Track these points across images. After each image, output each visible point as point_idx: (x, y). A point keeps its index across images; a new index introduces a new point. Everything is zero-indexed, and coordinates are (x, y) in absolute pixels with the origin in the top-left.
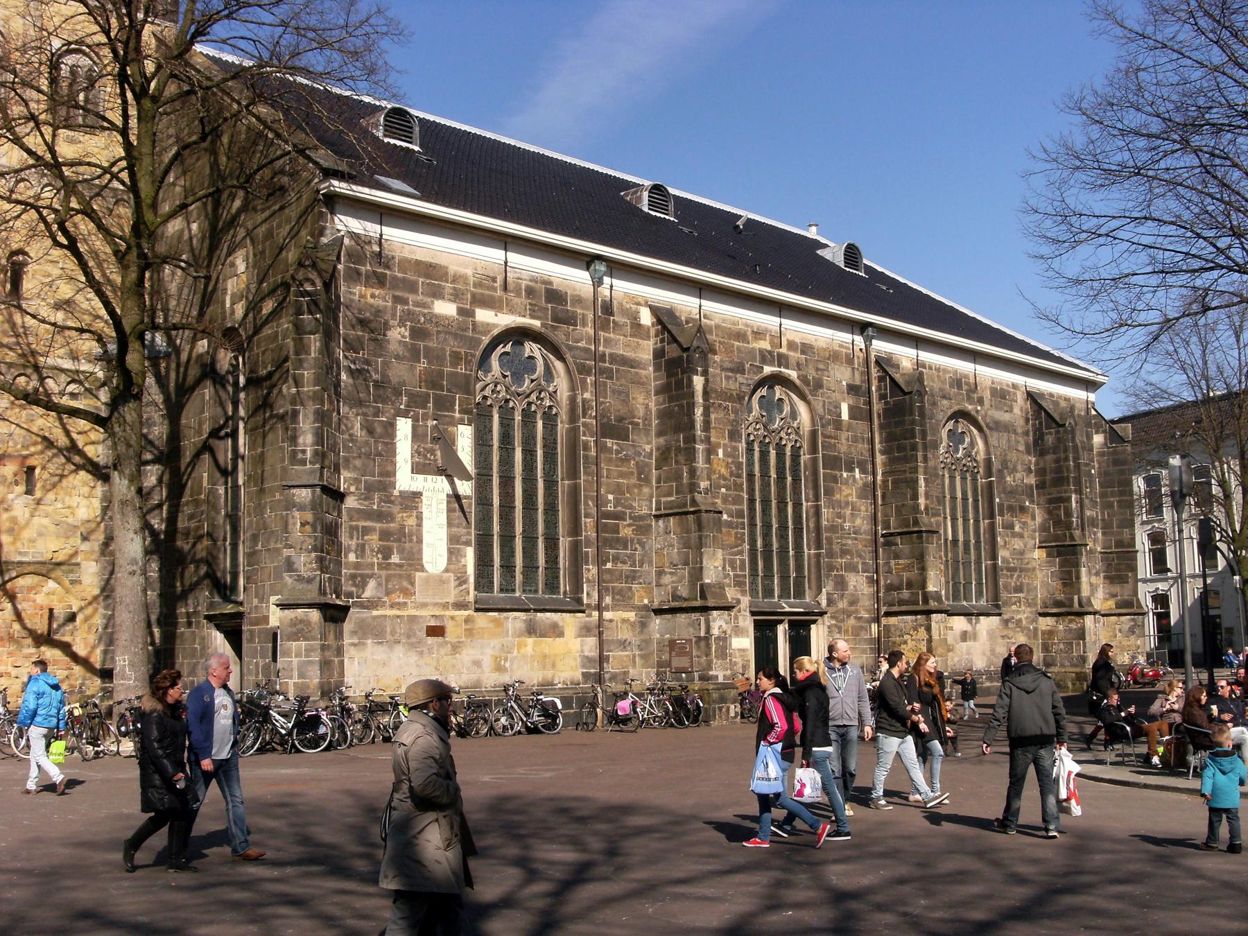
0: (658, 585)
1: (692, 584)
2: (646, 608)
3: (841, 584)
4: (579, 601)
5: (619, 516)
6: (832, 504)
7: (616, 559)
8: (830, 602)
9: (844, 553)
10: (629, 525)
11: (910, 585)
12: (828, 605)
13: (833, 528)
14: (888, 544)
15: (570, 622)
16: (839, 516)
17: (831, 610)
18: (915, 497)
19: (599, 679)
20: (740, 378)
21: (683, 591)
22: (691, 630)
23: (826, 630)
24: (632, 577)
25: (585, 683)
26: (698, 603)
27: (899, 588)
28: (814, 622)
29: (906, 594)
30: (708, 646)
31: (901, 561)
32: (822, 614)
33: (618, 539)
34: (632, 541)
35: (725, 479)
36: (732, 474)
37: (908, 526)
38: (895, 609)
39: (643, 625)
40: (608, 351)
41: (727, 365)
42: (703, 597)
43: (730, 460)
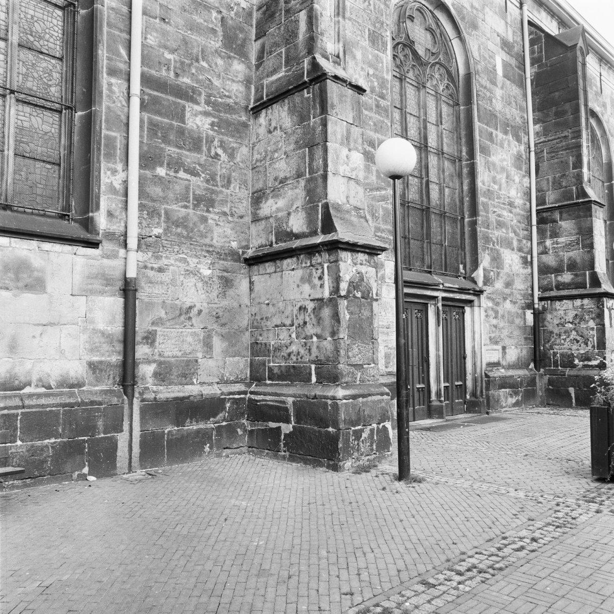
0: (256, 219)
1: (310, 211)
2: (234, 255)
3: (497, 260)
4: (88, 224)
5: (188, 95)
6: (489, 166)
7: (176, 165)
8: (487, 281)
9: (500, 225)
10: (206, 114)
11: (572, 266)
12: (485, 284)
14: (541, 221)
15: (64, 263)
18: (578, 164)
19: (127, 375)
21: (297, 223)
22: (306, 288)
23: (483, 314)
24: (206, 201)
25: (98, 381)
26: (320, 239)
27: (558, 270)
29: (567, 277)
30: (336, 317)
31: (561, 240)
32: (478, 293)
33: (181, 132)
34: (210, 141)
37: (571, 198)
38: (554, 293)
39: (227, 283)
42: (328, 226)
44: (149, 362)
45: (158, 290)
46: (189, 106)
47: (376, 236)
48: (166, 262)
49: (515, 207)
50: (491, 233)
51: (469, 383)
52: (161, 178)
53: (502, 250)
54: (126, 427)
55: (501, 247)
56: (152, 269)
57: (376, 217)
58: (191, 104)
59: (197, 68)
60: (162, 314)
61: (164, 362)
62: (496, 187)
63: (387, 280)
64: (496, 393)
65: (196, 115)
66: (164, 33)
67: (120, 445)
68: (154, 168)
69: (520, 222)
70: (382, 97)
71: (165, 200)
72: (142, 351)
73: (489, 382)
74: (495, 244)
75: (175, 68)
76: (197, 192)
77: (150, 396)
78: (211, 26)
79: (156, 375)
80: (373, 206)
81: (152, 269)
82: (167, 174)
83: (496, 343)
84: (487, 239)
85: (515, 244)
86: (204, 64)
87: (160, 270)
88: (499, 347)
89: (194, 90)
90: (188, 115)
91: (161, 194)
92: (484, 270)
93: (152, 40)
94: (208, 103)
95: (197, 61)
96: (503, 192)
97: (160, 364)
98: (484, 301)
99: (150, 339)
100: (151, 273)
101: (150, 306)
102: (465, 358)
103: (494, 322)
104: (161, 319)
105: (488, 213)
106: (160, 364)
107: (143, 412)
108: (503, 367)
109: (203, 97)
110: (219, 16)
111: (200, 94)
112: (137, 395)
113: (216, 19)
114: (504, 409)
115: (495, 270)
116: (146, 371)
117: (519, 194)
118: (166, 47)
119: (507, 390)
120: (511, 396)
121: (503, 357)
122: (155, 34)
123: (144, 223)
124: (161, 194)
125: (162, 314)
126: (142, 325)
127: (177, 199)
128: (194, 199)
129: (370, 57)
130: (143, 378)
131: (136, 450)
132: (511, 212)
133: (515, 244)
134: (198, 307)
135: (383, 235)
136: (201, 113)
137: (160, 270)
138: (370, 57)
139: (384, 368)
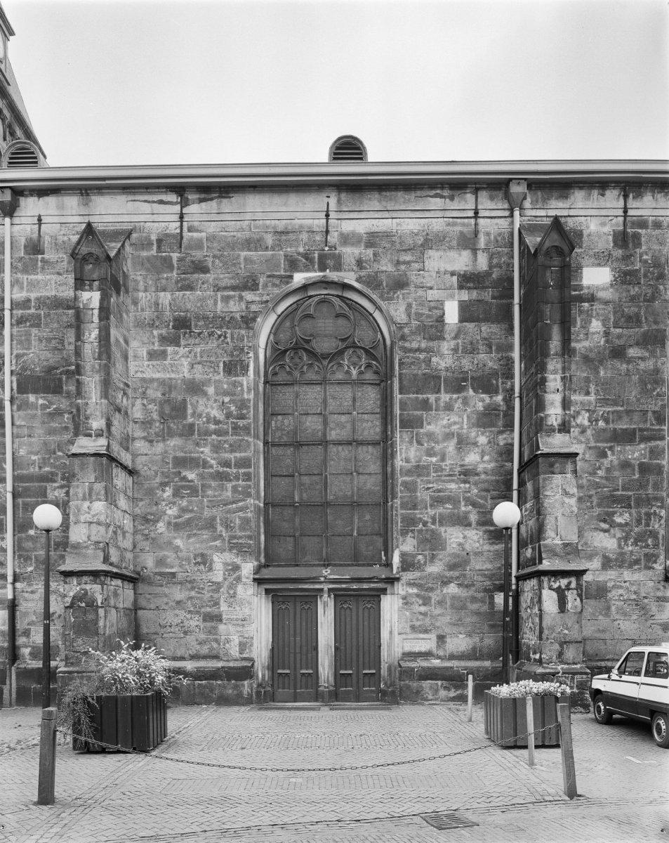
3: (432, 543)
8: (407, 565)
9: (438, 501)
13: (419, 470)
16: (430, 453)
17: (408, 576)
20: (249, 296)
28: (384, 591)
32: (392, 581)
35: (217, 422)
36: (229, 415)
40: (33, 296)
41: (227, 281)
43: (227, 399)
44: (26, 647)
45: (30, 605)
46: (49, 486)
47: (231, 543)
48: (35, 587)
49: (477, 474)
50: (421, 514)
51: (384, 672)
52: (31, 537)
53: (443, 529)
54: (8, 682)
55: (441, 524)
56: (27, 592)
57: (231, 527)
58: (51, 484)
59: (55, 458)
60: (34, 619)
61: (36, 647)
62: (434, 459)
63: (244, 580)
64: (415, 685)
65: (55, 490)
66: (30, 444)
67: (5, 691)
68: (27, 531)
69: (487, 491)
70: (242, 417)
71: (35, 549)
72: (21, 640)
73: (407, 673)
74: (429, 524)
75: (39, 463)
76: (57, 540)
77: (22, 666)
78: (64, 425)
79: (31, 654)
80: (227, 518)
81: (27, 592)
82: (35, 533)
83: (426, 631)
84: (410, 522)
85: (473, 517)
86: (60, 454)
87: (32, 592)
88: (433, 636)
89: (52, 473)
90: (48, 491)
91: (32, 546)
92: (403, 555)
93: (22, 452)
94: (63, 479)
95: (55, 453)
96: (448, 462)
97: (33, 648)
98: (400, 589)
99: (27, 633)
100: (26, 595)
101: (26, 614)
102: (380, 647)
103: (423, 609)
104: (33, 621)
105: (415, 491)
106: (33, 648)
107: (18, 675)
108: (439, 657)
109: (60, 476)
110: (70, 416)
111: (57, 475)
112: (15, 665)
113: (67, 419)
114: (430, 702)
115: (427, 553)
116: (26, 651)
117: (486, 458)
118: (31, 453)
119: (439, 683)
120: (446, 688)
121: (438, 647)
122: (25, 447)
123: (22, 566)
124: (32, 546)
125: (34, 619)
126: (20, 626)
127: (42, 548)
128: (55, 545)
129: (225, 386)
130: (23, 656)
131: (14, 695)
132: (465, 482)
133: (473, 517)
134: (59, 612)
135: (240, 541)
136: (58, 487)
137: (32, 592)
138: (225, 386)
139: (237, 654)
